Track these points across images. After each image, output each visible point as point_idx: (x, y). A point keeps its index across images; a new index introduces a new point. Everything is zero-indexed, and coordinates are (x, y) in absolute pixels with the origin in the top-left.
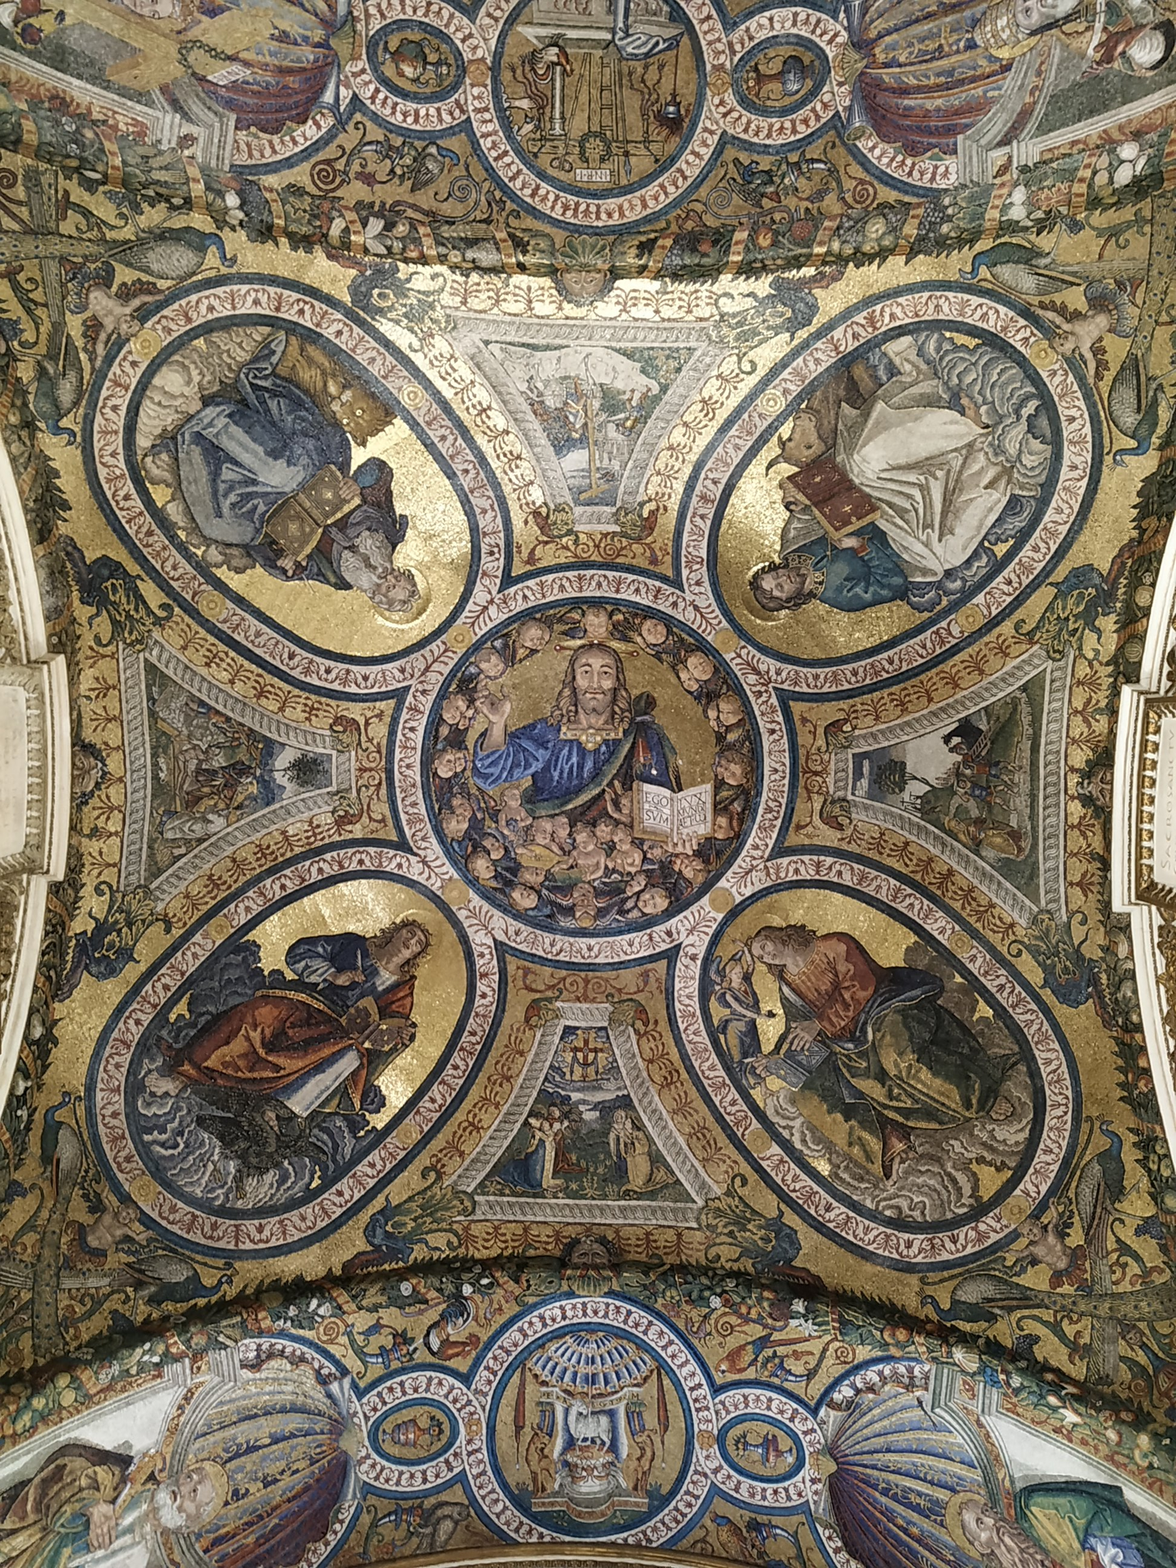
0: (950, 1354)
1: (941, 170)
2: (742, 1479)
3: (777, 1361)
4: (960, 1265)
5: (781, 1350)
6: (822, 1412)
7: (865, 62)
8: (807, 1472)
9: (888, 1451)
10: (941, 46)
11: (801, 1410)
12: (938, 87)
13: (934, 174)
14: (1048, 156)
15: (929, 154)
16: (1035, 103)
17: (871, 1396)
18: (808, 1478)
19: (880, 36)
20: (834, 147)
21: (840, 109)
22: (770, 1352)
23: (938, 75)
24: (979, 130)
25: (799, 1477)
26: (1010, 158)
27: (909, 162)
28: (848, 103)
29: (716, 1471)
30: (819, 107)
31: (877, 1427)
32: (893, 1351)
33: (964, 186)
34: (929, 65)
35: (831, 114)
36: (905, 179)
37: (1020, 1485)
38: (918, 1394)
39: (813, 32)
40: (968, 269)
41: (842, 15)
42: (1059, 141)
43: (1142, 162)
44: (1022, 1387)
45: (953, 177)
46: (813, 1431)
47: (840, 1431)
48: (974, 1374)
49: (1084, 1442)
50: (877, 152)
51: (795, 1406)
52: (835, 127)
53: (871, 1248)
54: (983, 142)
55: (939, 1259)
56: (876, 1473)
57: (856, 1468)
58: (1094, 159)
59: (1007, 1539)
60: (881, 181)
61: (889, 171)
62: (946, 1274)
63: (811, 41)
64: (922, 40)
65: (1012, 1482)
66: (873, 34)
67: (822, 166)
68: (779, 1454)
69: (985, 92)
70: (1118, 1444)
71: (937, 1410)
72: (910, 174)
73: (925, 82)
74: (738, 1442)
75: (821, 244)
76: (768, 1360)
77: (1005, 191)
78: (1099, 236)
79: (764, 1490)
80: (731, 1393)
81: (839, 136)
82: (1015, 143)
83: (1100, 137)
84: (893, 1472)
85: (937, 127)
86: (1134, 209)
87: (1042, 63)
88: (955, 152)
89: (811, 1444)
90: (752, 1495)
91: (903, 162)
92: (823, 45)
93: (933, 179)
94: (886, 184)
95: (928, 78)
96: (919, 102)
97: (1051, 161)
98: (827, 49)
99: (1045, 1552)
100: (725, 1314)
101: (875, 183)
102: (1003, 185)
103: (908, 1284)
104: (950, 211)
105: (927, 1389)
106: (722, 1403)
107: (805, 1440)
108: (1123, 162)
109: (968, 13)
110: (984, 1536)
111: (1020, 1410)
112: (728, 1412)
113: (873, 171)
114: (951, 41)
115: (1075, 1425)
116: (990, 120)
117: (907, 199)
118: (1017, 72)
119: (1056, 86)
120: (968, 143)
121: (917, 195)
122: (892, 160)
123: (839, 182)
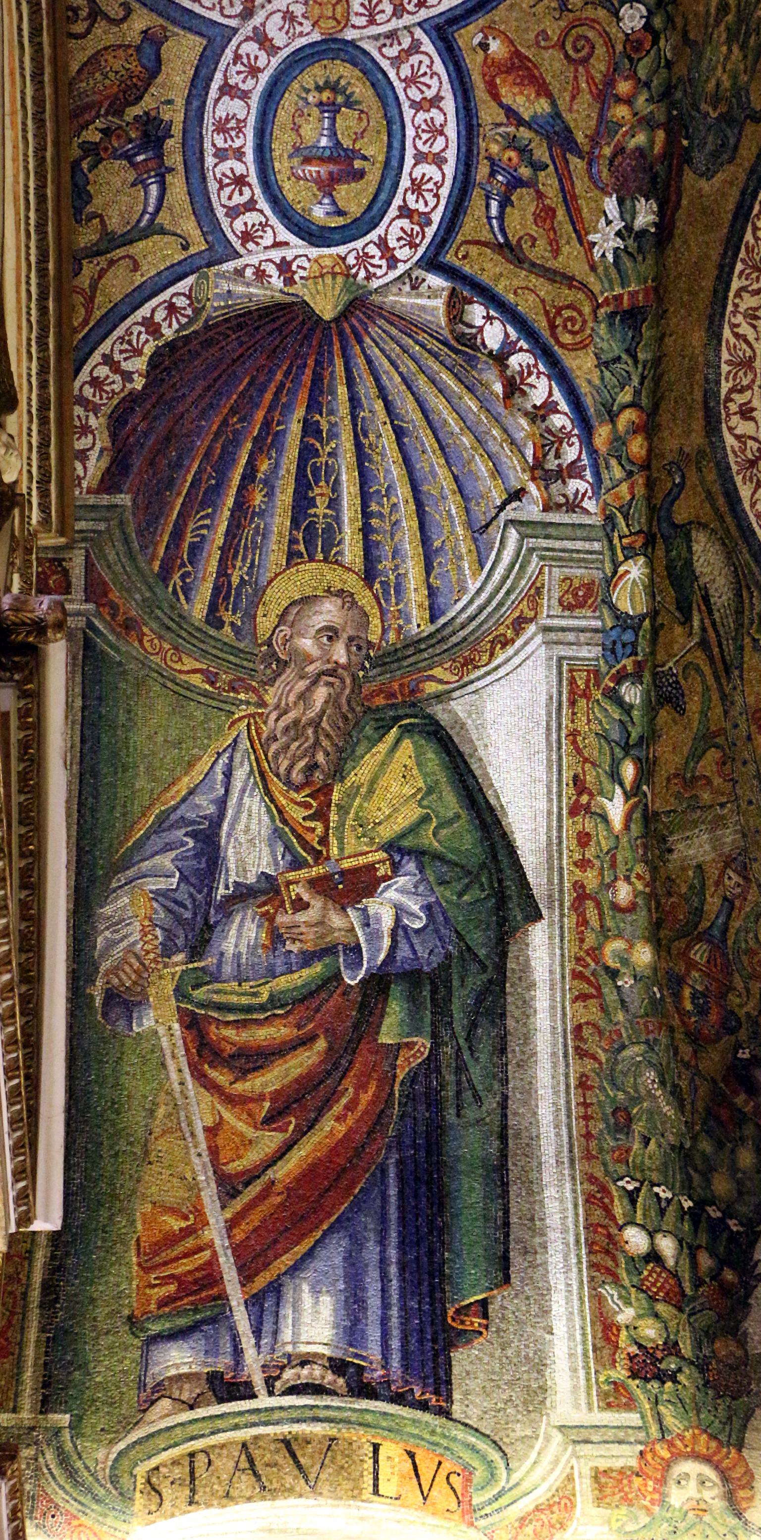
0: (630, 553)
2: (255, 101)
3: (525, 172)
4: (739, 526)
5: (549, 182)
6: (435, 281)
8: (297, 247)
9: (399, 433)
11: (430, 231)
17: (498, 388)
18: (289, 254)
22: (541, 153)
25: (284, 235)
29: (262, 39)
31: (437, 403)
32: (602, 434)
37: (439, 711)
38: (532, 488)
44: (627, 709)
46: (393, 262)
47: (397, 318)
48: (613, 607)
49: (584, 839)
51: (436, 217)
53: (727, 333)
55: (738, 479)
56: (343, 408)
57: (339, 363)
59: (321, 694)
62: (721, 501)
65: (439, 697)
68: (327, 186)
70: (615, 907)
71: (513, 534)
74: (333, 87)
76: (524, 151)
79: (239, 154)
80: (439, 67)
84: (358, 446)
89: (363, 258)
90: (221, 128)
99: (338, 772)
100: (609, 42)
103: (688, 433)
105: (546, 509)
106: (415, 48)
107: (366, 243)
110: (307, 644)
111: (582, 703)
112: (397, 62)
115: (604, 818)
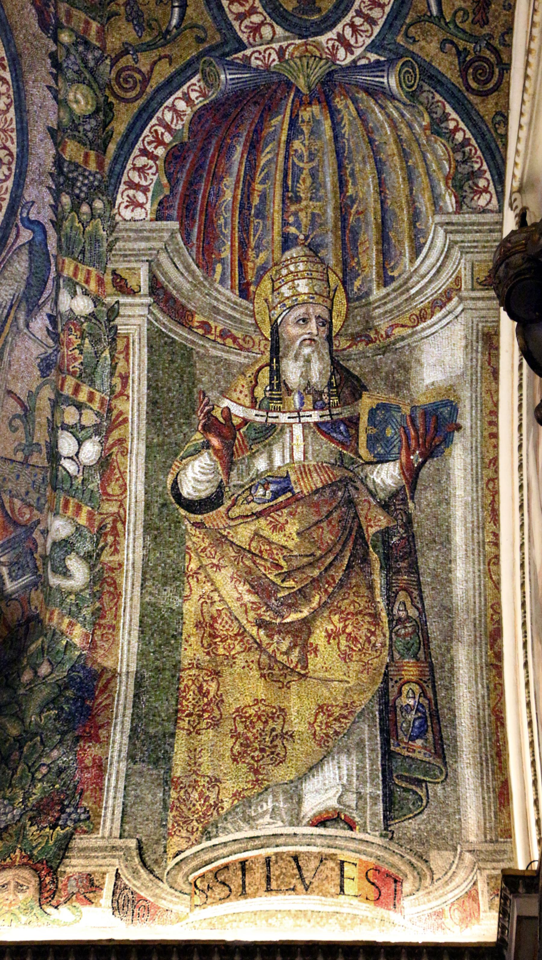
1: (141, 198)
7: (305, 91)
10: (298, 200)
12: (247, 195)
13: (136, 187)
14: (120, 345)
15: (165, 181)
16: (190, 328)
19: (333, 112)
20: (200, 40)
21: (248, 52)
23: (263, 197)
24: (177, 251)
26: (132, 293)
27: (160, 151)
28: (255, 63)
30: (256, 19)
33: (113, 228)
34: (278, 183)
35: (244, 37)
36: (139, 145)
39: (359, 13)
40: (32, 217)
41: (373, 57)
42: (134, 360)
43: (70, 466)
45: (127, 214)
50: (181, 105)
52: (225, 42)
54: (163, 258)
58: (96, 406)
60: (142, 110)
61: (154, 121)
63: (347, 10)
64: (313, 174)
66: (339, 103)
67: (174, 22)
69: (222, 261)
72: (144, 152)
73: (259, 178)
75: (69, 15)
77: (93, 286)
78: (31, 395)
81: (212, 49)
82: (149, 300)
83: (121, 413)
85: (196, 192)
86: (42, 443)
87: (235, 339)
88: (158, 218)
91: (160, 142)
92: (339, 28)
93: (132, 185)
94: (138, 117)
95: (263, 182)
96: (235, 169)
97: (113, 350)
98: (332, 34)
101: (140, 102)
102: (100, 282)
104: (85, 208)
108: (80, 443)
109: (330, 238)
113: (158, 99)
114: (302, 215)
116: (187, 268)
117: (112, 147)
118: (235, 306)
119: (202, 358)
120: (166, 236)
121: (115, 159)
122: (167, 127)
123: (149, 47)
